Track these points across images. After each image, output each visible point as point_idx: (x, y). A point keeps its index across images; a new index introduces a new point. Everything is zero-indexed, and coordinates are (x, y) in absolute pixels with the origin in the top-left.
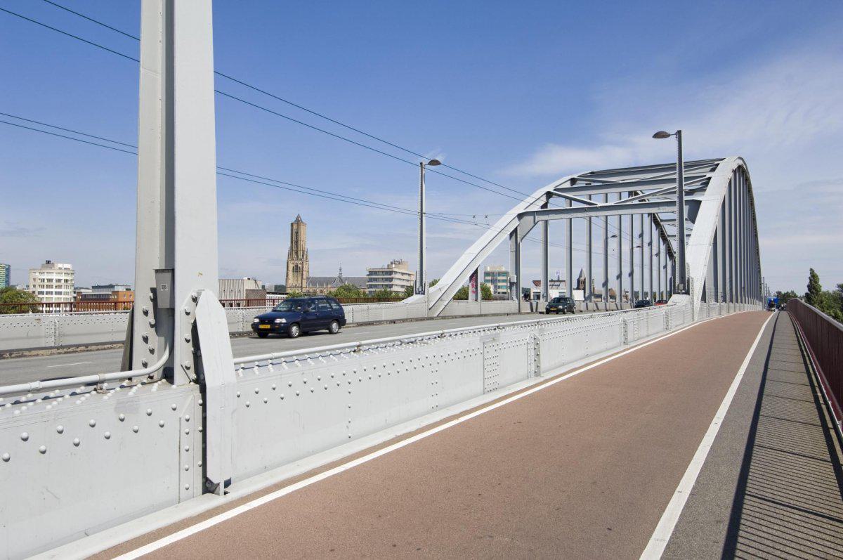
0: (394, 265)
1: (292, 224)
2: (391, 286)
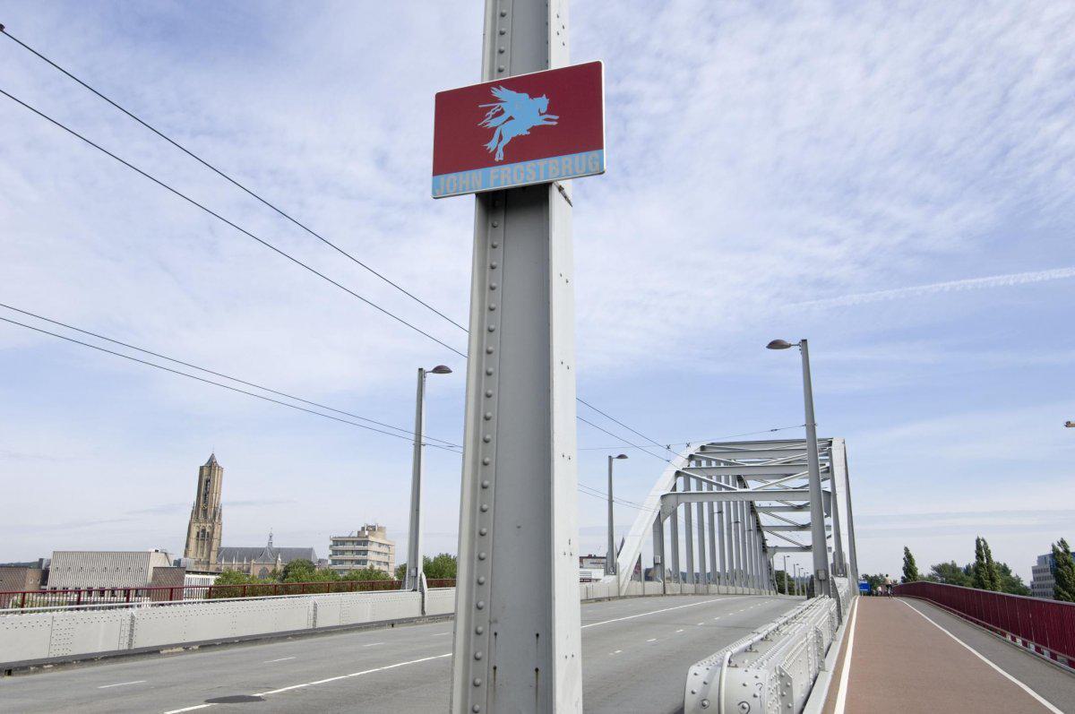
0: (367, 533)
1: (202, 468)
2: (365, 562)
